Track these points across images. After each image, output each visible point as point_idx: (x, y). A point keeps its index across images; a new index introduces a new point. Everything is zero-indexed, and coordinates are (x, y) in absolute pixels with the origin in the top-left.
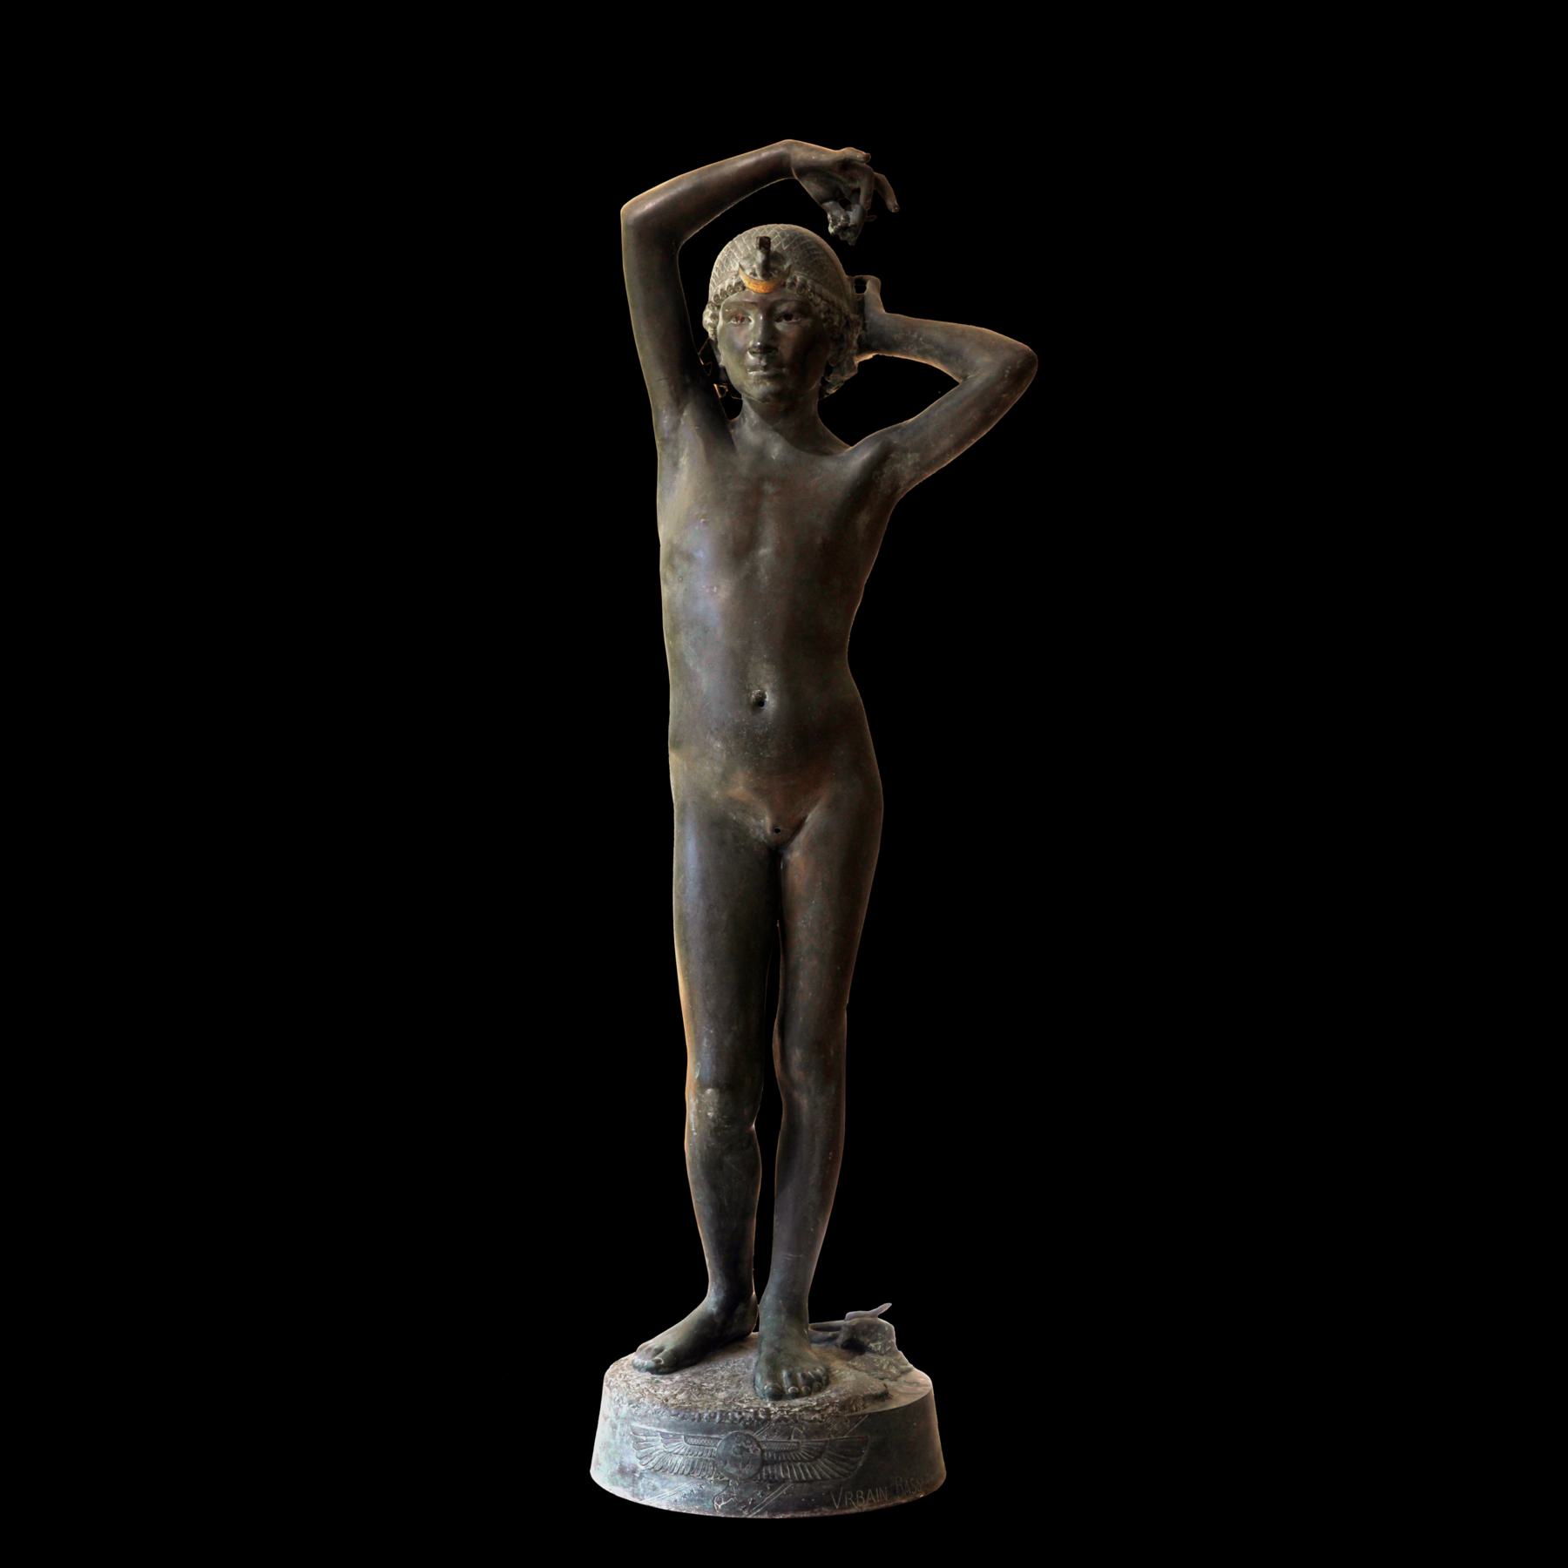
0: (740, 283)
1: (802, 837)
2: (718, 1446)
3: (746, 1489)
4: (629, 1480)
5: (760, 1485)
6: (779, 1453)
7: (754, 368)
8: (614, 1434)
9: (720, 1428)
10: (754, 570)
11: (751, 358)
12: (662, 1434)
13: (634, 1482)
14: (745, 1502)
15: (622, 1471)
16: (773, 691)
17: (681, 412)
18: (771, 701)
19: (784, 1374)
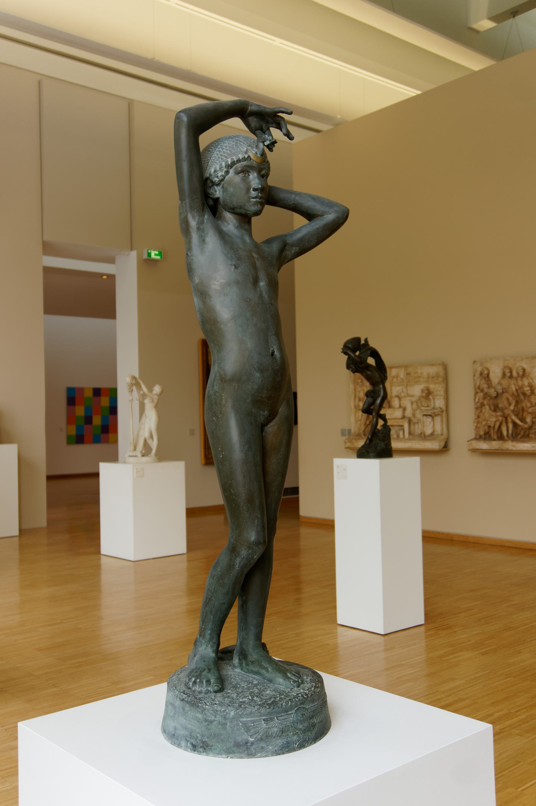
0: (249, 157)
1: (277, 419)
2: (292, 717)
3: (305, 733)
4: (245, 748)
5: (309, 730)
6: (313, 711)
7: (254, 198)
8: (225, 729)
9: (291, 708)
10: (261, 292)
11: (253, 193)
12: (264, 720)
13: (248, 749)
14: (306, 740)
15: (237, 745)
16: (278, 349)
17: (204, 216)
18: (277, 353)
19: (289, 675)
